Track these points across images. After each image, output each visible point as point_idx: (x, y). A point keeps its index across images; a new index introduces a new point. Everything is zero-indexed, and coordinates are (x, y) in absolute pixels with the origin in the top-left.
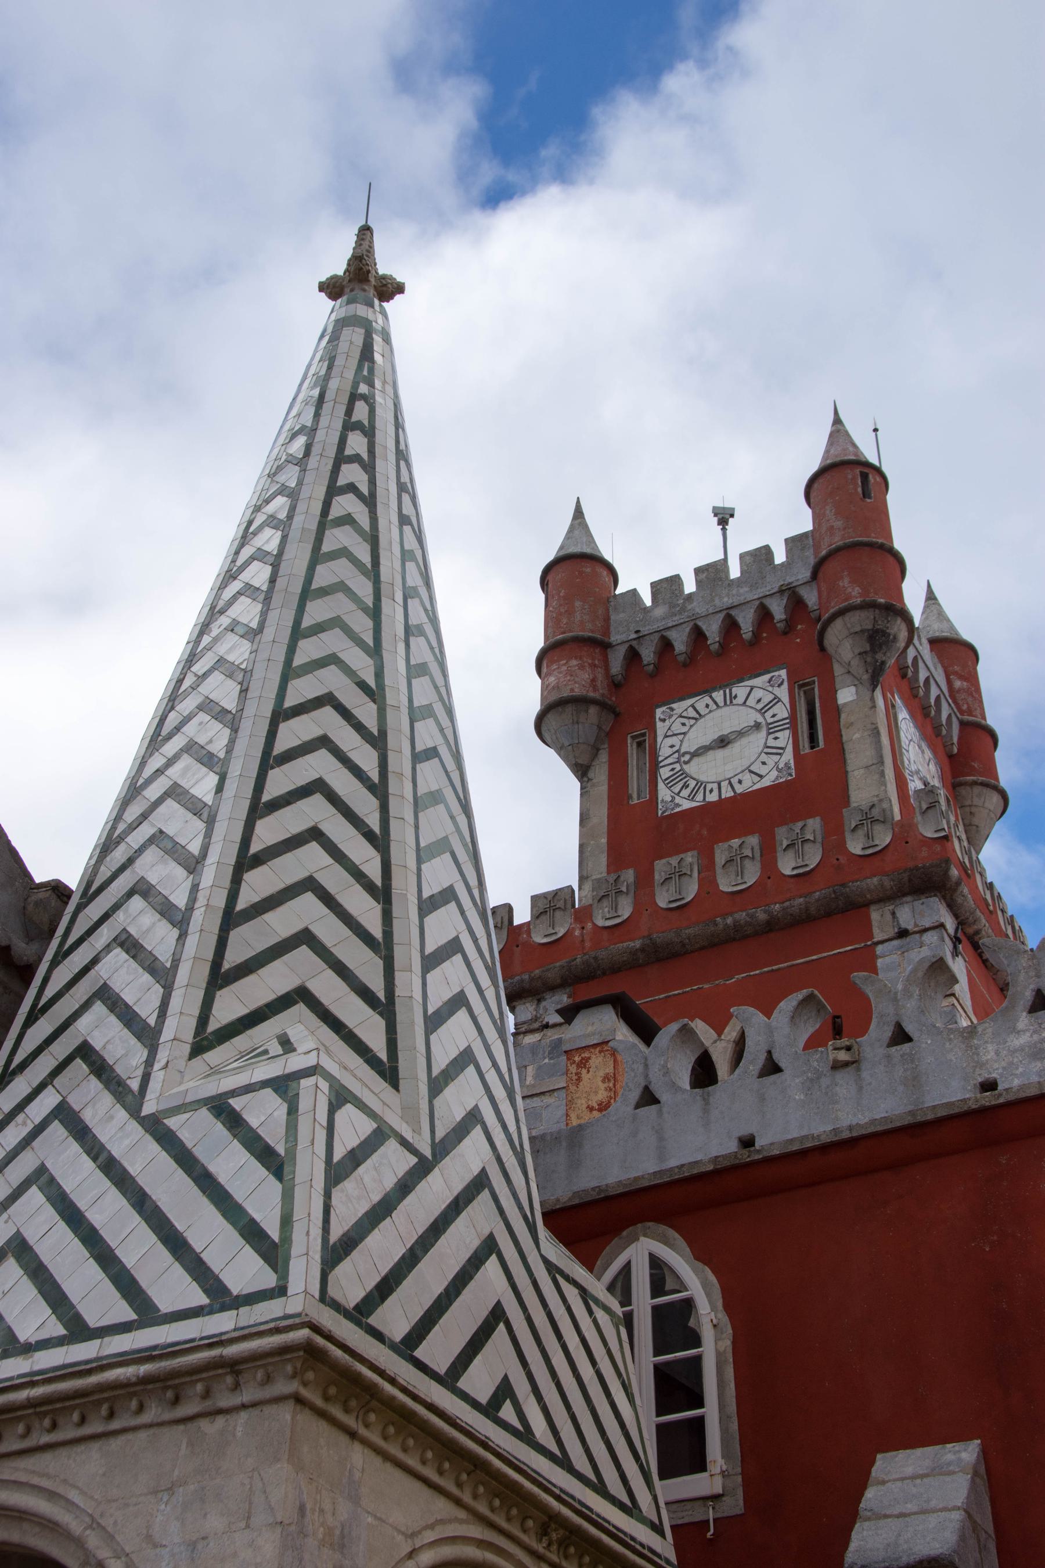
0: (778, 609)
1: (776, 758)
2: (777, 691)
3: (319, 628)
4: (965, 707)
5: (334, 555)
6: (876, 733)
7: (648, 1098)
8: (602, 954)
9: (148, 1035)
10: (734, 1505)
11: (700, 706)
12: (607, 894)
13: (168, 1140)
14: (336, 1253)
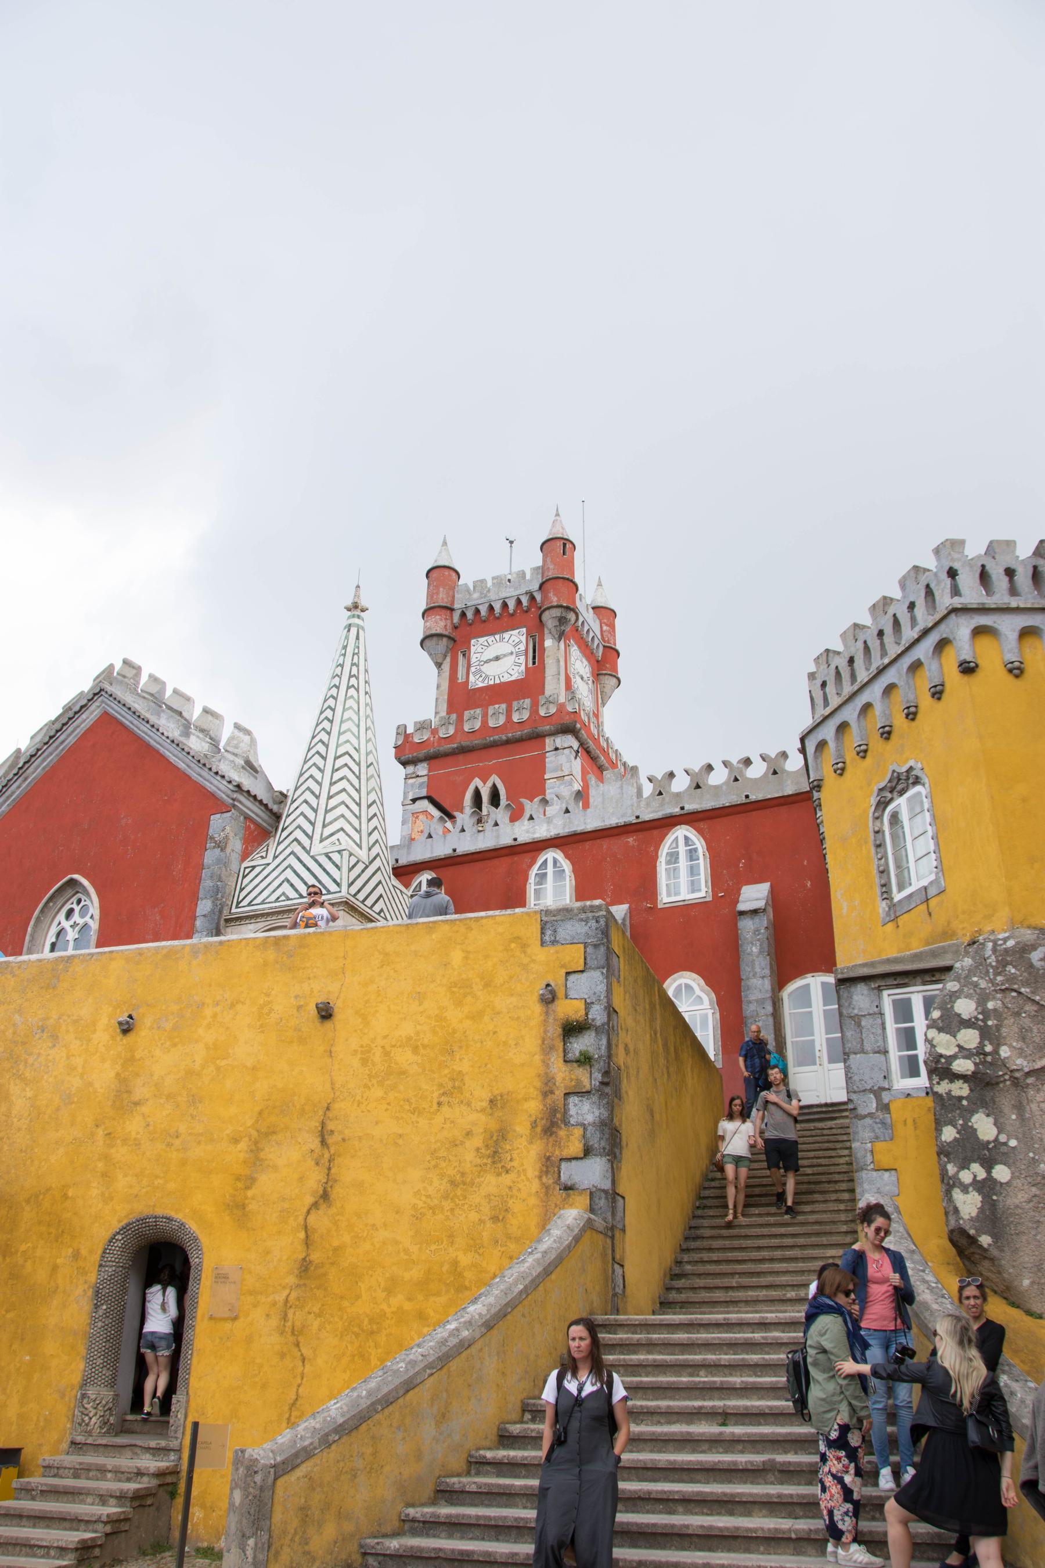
0: (525, 601)
3: (345, 732)
5: (348, 709)
6: (558, 661)
7: (430, 836)
8: (441, 749)
9: (311, 838)
11: (490, 641)
12: (445, 723)
13: (316, 861)
14: (350, 885)
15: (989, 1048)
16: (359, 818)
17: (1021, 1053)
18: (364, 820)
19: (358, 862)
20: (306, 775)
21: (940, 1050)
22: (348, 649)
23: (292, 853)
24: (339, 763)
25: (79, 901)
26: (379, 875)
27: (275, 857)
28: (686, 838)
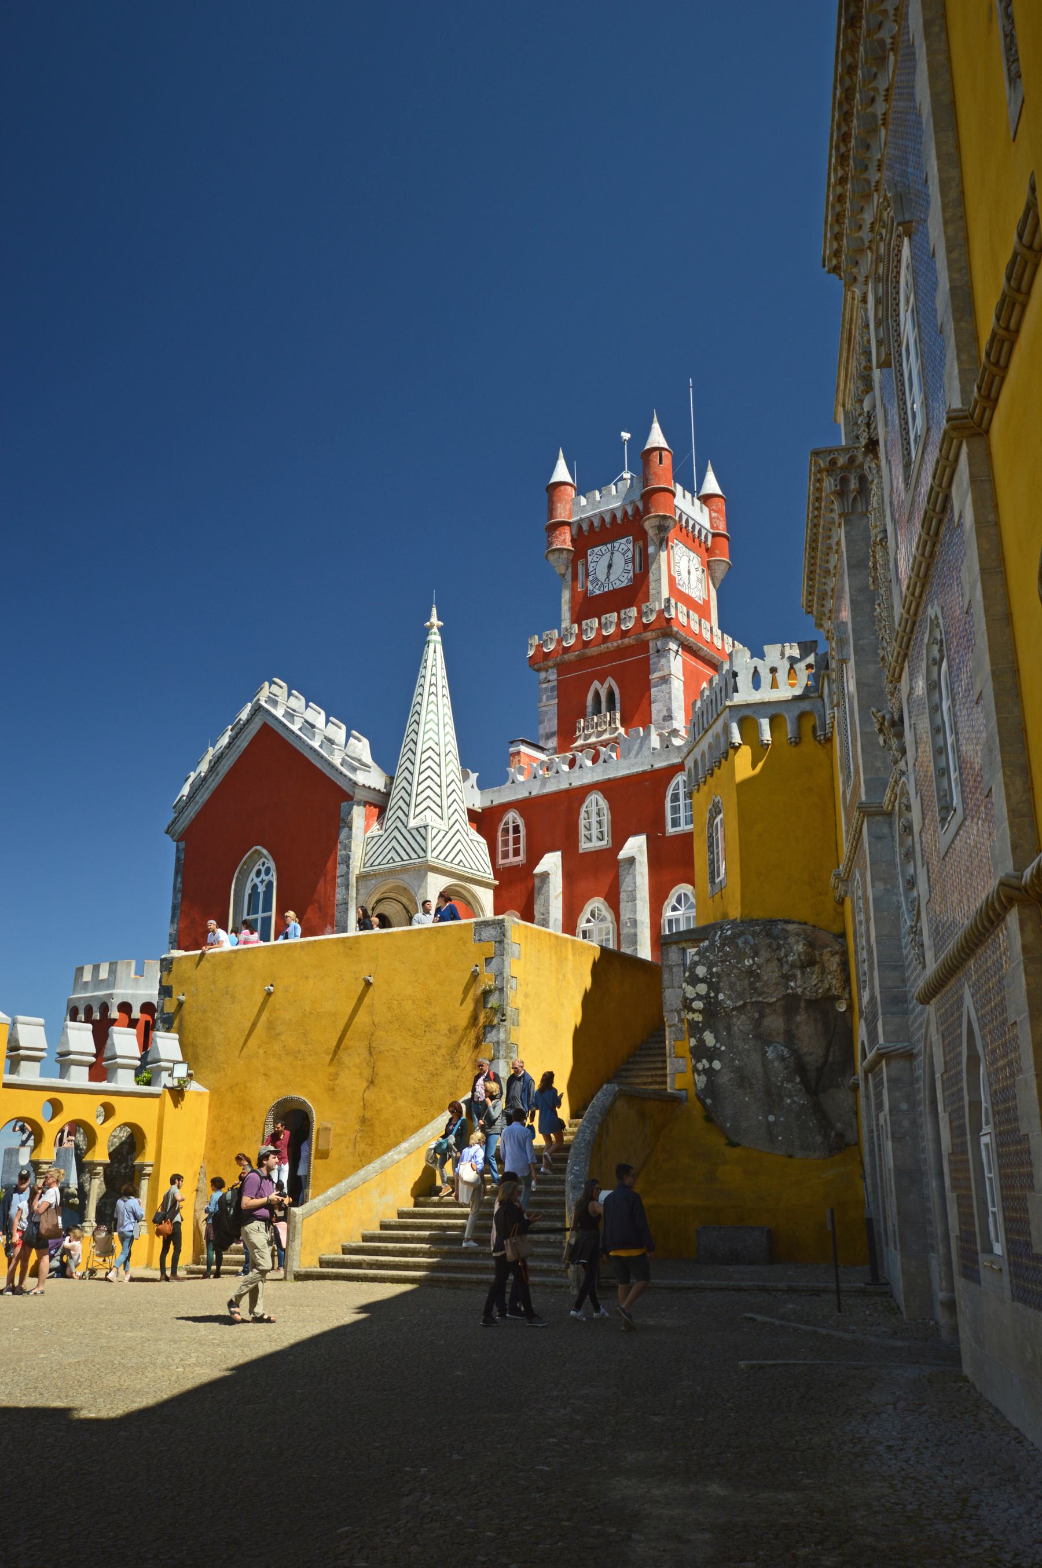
10: (524, 862)
15: (712, 995)
16: (440, 796)
17: (729, 997)
18: (444, 797)
20: (403, 767)
21: (688, 995)
23: (396, 827)
25: (264, 864)
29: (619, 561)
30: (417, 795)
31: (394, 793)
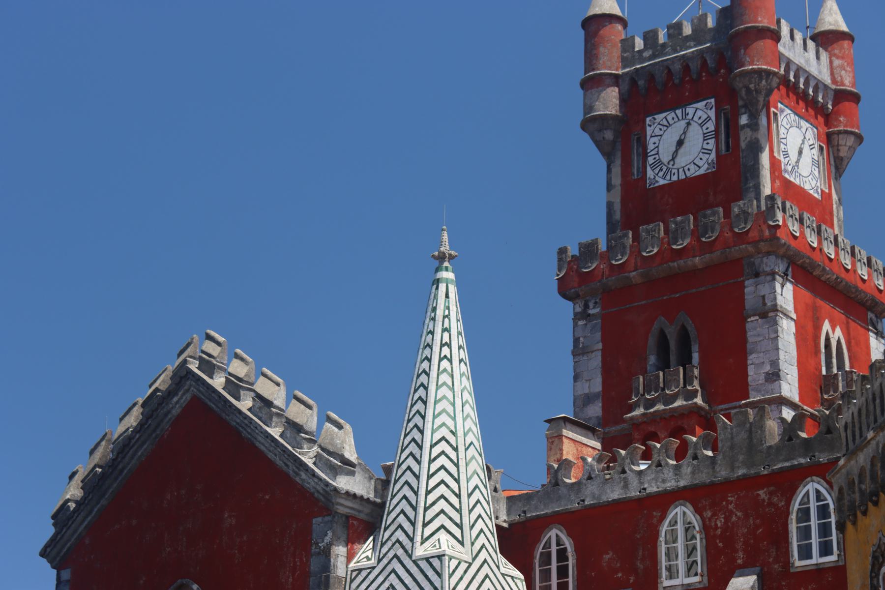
1: (707, 156)
2: (709, 112)
3: (439, 414)
4: (839, 79)
11: (669, 118)
13: (418, 566)
16: (459, 511)
18: (465, 512)
19: (459, 564)
20: (404, 467)
22: (438, 312)
23: (396, 556)
24: (436, 451)
26: (485, 570)
27: (379, 560)
28: (818, 491)
29: (695, 136)
30: (426, 509)
31: (391, 504)
